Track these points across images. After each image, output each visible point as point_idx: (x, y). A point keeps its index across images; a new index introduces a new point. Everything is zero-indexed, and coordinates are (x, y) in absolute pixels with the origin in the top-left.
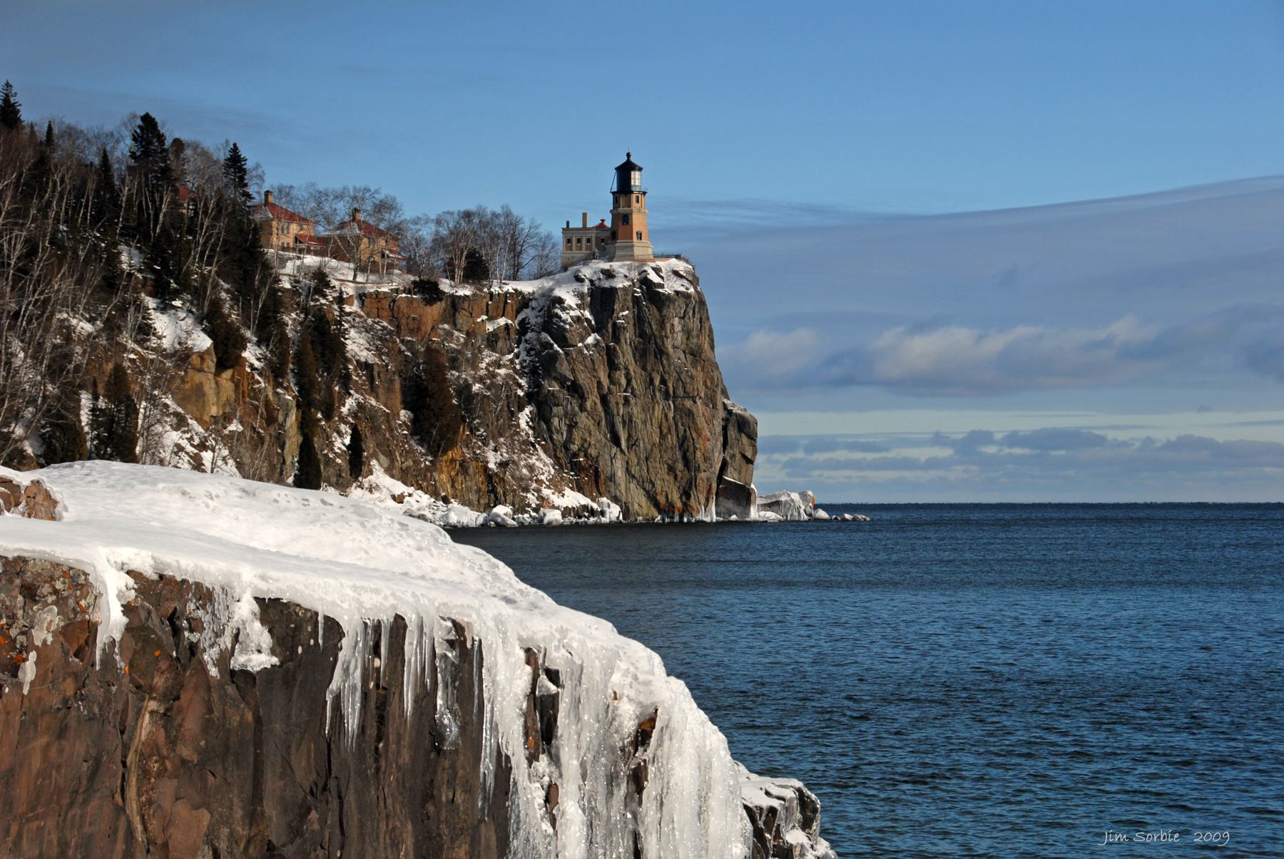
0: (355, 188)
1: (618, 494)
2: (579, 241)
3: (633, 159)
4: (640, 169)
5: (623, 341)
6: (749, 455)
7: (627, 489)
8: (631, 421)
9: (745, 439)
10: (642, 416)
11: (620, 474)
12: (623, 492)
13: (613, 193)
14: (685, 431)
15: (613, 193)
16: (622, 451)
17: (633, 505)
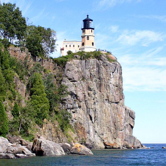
0: (4, 4)
1: (91, 139)
2: (70, 46)
4: (92, 20)
6: (132, 125)
7: (94, 137)
8: (95, 110)
9: (131, 119)
10: (99, 109)
11: (91, 131)
12: (93, 138)
13: (82, 29)
14: (115, 115)
15: (82, 29)
16: (92, 122)
17: (96, 143)
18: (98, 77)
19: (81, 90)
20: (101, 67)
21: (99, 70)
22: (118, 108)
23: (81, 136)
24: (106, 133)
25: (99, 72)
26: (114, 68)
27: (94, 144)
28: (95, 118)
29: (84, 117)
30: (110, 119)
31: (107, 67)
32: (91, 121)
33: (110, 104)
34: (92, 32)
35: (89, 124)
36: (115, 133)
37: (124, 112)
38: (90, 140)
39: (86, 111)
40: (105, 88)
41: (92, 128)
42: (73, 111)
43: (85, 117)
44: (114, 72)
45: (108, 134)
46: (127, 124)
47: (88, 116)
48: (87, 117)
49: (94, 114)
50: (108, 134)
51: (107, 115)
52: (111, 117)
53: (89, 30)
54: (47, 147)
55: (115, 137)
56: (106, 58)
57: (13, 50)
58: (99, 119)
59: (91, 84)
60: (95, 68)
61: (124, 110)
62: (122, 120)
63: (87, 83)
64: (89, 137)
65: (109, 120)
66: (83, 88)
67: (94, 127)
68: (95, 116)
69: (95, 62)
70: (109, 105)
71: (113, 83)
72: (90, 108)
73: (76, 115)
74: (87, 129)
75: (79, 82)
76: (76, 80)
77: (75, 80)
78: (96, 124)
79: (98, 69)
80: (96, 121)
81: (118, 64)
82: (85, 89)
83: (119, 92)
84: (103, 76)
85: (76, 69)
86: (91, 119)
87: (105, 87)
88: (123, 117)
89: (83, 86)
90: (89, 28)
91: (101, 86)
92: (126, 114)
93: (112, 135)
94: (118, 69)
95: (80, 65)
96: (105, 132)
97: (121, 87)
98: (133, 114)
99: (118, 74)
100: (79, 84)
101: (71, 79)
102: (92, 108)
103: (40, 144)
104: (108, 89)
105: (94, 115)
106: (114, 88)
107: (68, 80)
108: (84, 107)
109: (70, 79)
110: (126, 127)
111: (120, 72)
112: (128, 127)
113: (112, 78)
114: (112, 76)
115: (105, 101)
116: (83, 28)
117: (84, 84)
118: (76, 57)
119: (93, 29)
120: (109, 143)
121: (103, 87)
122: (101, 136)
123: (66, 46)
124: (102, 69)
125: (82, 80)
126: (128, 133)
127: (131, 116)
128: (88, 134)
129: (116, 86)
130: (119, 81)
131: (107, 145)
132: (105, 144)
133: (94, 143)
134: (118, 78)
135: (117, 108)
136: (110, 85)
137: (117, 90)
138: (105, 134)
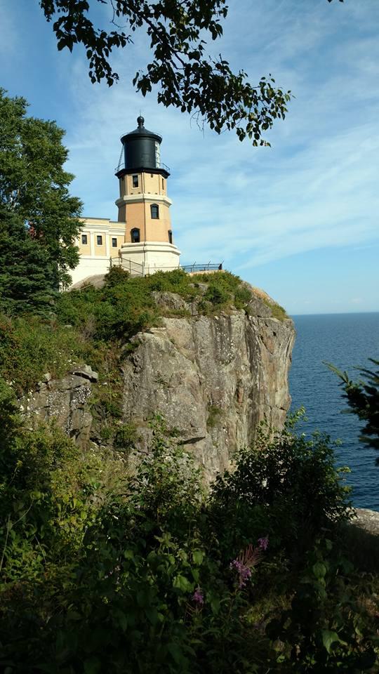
84: (263, 382)
101: (182, 433)
129: (281, 408)
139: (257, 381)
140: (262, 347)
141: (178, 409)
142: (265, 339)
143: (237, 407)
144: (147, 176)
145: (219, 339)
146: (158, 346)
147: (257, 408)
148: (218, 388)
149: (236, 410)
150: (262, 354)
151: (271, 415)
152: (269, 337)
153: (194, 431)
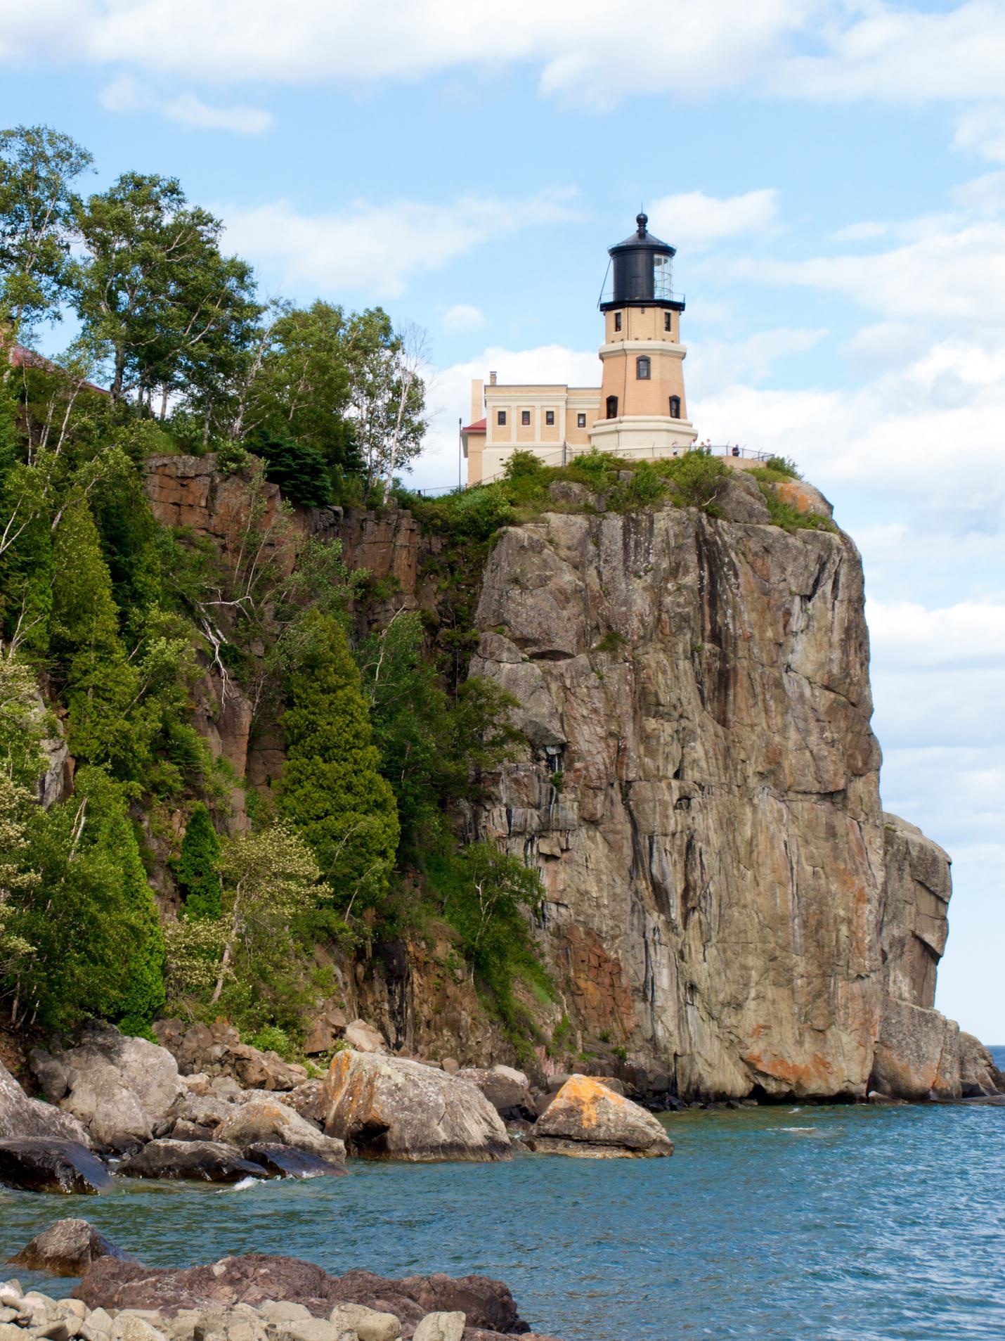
2: (526, 417)
3: (654, 230)
4: (668, 251)
5: (680, 648)
6: (930, 938)
7: (682, 1020)
8: (690, 846)
9: (927, 903)
10: (716, 840)
11: (664, 979)
14: (814, 873)
15: (605, 307)
16: (670, 924)
17: (692, 1060)
18: (708, 627)
19: (595, 711)
20: (732, 565)
21: (713, 582)
22: (840, 830)
23: (593, 1013)
24: (760, 997)
25: (714, 599)
26: (814, 568)
27: (683, 1067)
28: (685, 896)
29: (618, 891)
30: (786, 902)
31: (769, 560)
32: (663, 917)
33: (782, 806)
34: (668, 328)
35: (649, 935)
36: (818, 995)
37: (876, 857)
38: (653, 1040)
39: (628, 851)
40: (751, 702)
41: (664, 961)
42: (545, 849)
43: (621, 888)
44: (809, 598)
45: (774, 1002)
46: (896, 932)
47: (643, 885)
48: (636, 893)
49: (680, 867)
50: (774, 1002)
51: (767, 876)
52: (790, 889)
53: (649, 311)
54: (411, 1100)
55: (819, 1023)
56: (758, 506)
57: (172, 471)
58: (715, 902)
59: (664, 673)
60: (686, 572)
61: (878, 842)
62: (869, 907)
63: (637, 667)
64: (647, 1024)
65: (779, 911)
66: (611, 701)
67: (682, 957)
68: (687, 880)
69: (691, 531)
70: (779, 811)
71: (809, 668)
72: (658, 830)
73: (562, 876)
74: (632, 971)
75: (583, 659)
76: (567, 650)
77: (559, 644)
78: (693, 935)
79: (706, 574)
80: (695, 916)
81: (836, 539)
82: (626, 707)
83: (842, 724)
84: (743, 623)
85: (568, 578)
86: (663, 906)
87: (755, 696)
88: (874, 894)
89: (613, 688)
90: (649, 302)
91: (726, 688)
92: (894, 873)
93: (796, 1009)
94: (837, 573)
95: (591, 548)
96: (753, 994)
97: (860, 695)
98: (936, 872)
99: (841, 611)
100: (580, 673)
101: (535, 642)
102: (671, 828)
103: (370, 1083)
104: (772, 703)
105: (680, 876)
106: (813, 695)
107: (513, 646)
108: (619, 827)
109: (523, 642)
110: (890, 957)
111: (854, 594)
112: (907, 957)
113: (802, 637)
114: (797, 623)
115: (753, 781)
116: (609, 298)
117: (617, 676)
118: (566, 495)
119: (679, 307)
120: (782, 1062)
121: (739, 694)
122: (729, 1019)
123: (502, 418)
124: (736, 576)
125: (602, 648)
126: (906, 995)
127: (921, 883)
128: (640, 1006)
129: (827, 688)
130: (845, 652)
131: (765, 1075)
132: (750, 1065)
133: (683, 1061)
134: (837, 636)
135: (832, 832)
136: (785, 680)
137: (831, 710)
138: (751, 1004)
139: (729, 620)
140: (743, 568)
141: (532, 613)
142: (750, 558)
143: (662, 642)
144: (635, 312)
145: (632, 544)
146: (518, 541)
147: (732, 663)
148: (624, 609)
149: (659, 646)
150: (741, 580)
151: (761, 678)
152: (755, 554)
153: (550, 641)
